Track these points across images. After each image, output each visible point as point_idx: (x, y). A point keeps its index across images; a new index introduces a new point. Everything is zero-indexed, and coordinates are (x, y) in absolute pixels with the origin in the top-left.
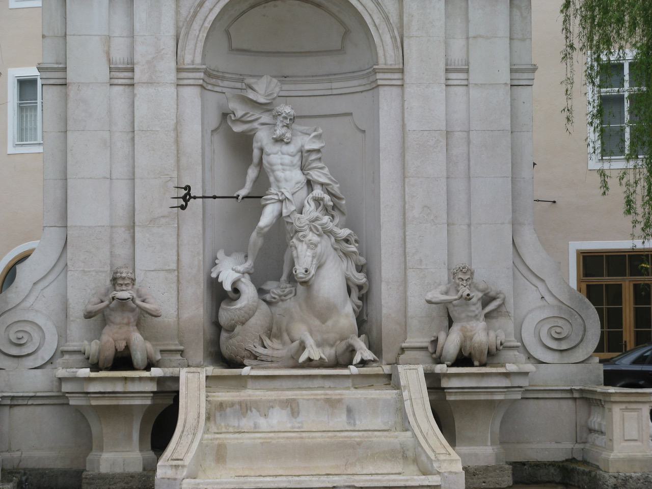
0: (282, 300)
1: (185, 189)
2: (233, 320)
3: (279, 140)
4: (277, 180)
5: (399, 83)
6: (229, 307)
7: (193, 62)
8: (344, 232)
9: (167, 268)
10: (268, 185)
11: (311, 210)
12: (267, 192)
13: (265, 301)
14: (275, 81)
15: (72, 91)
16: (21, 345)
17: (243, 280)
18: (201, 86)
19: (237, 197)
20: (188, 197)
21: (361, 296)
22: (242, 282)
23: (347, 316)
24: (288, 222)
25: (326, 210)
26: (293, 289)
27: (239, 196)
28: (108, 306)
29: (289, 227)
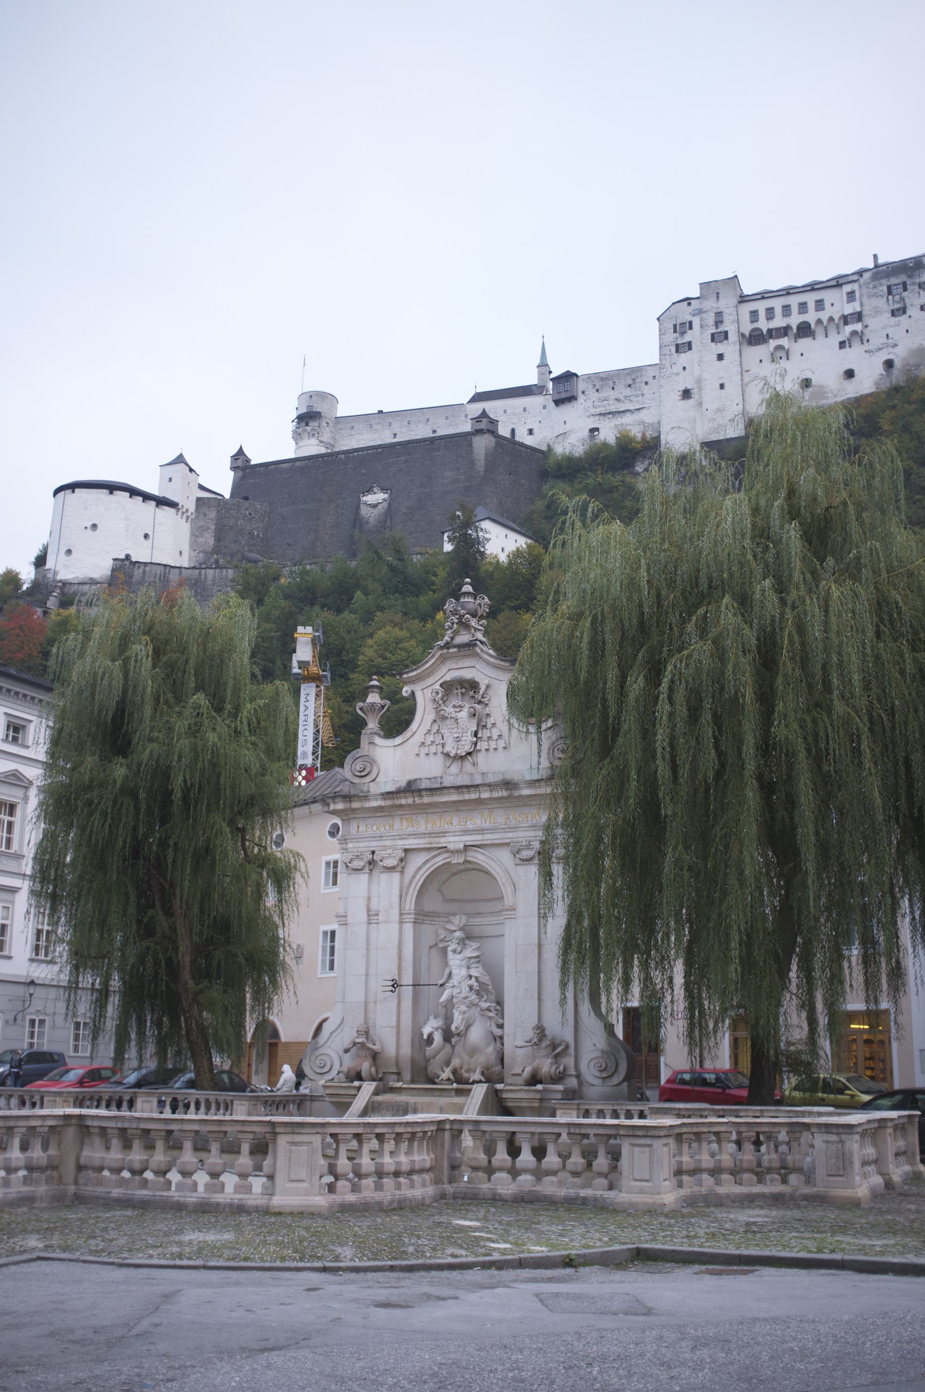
3: (454, 951)
8: (485, 1005)
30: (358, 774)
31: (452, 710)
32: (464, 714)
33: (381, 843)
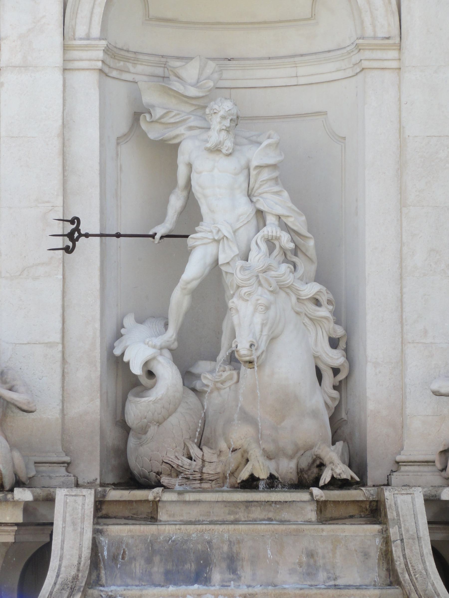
0: (218, 389)
1: (72, 222)
2: (145, 418)
4: (212, 211)
5: (394, 64)
6: (138, 399)
7: (88, 38)
10: (198, 218)
12: (197, 229)
13: (194, 390)
17: (160, 359)
18: (101, 70)
19: (153, 236)
20: (76, 235)
21: (338, 384)
22: (159, 362)
23: (315, 414)
24: (226, 273)
26: (235, 373)
27: (156, 234)
29: (227, 280)
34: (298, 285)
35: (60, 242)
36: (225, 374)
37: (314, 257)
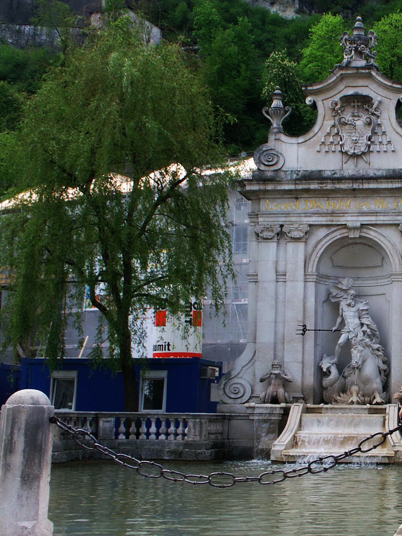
0: (349, 376)
1: (303, 326)
3: (349, 305)
4: (348, 323)
8: (376, 346)
9: (298, 361)
11: (361, 335)
14: (351, 280)
15: (260, 284)
16: (237, 393)
17: (332, 367)
19: (332, 331)
25: (369, 336)
28: (269, 377)
30: (266, 163)
31: (351, 118)
32: (359, 123)
33: (288, 219)
34: (372, 345)
35: (302, 332)
36: (351, 372)
37: (379, 338)
